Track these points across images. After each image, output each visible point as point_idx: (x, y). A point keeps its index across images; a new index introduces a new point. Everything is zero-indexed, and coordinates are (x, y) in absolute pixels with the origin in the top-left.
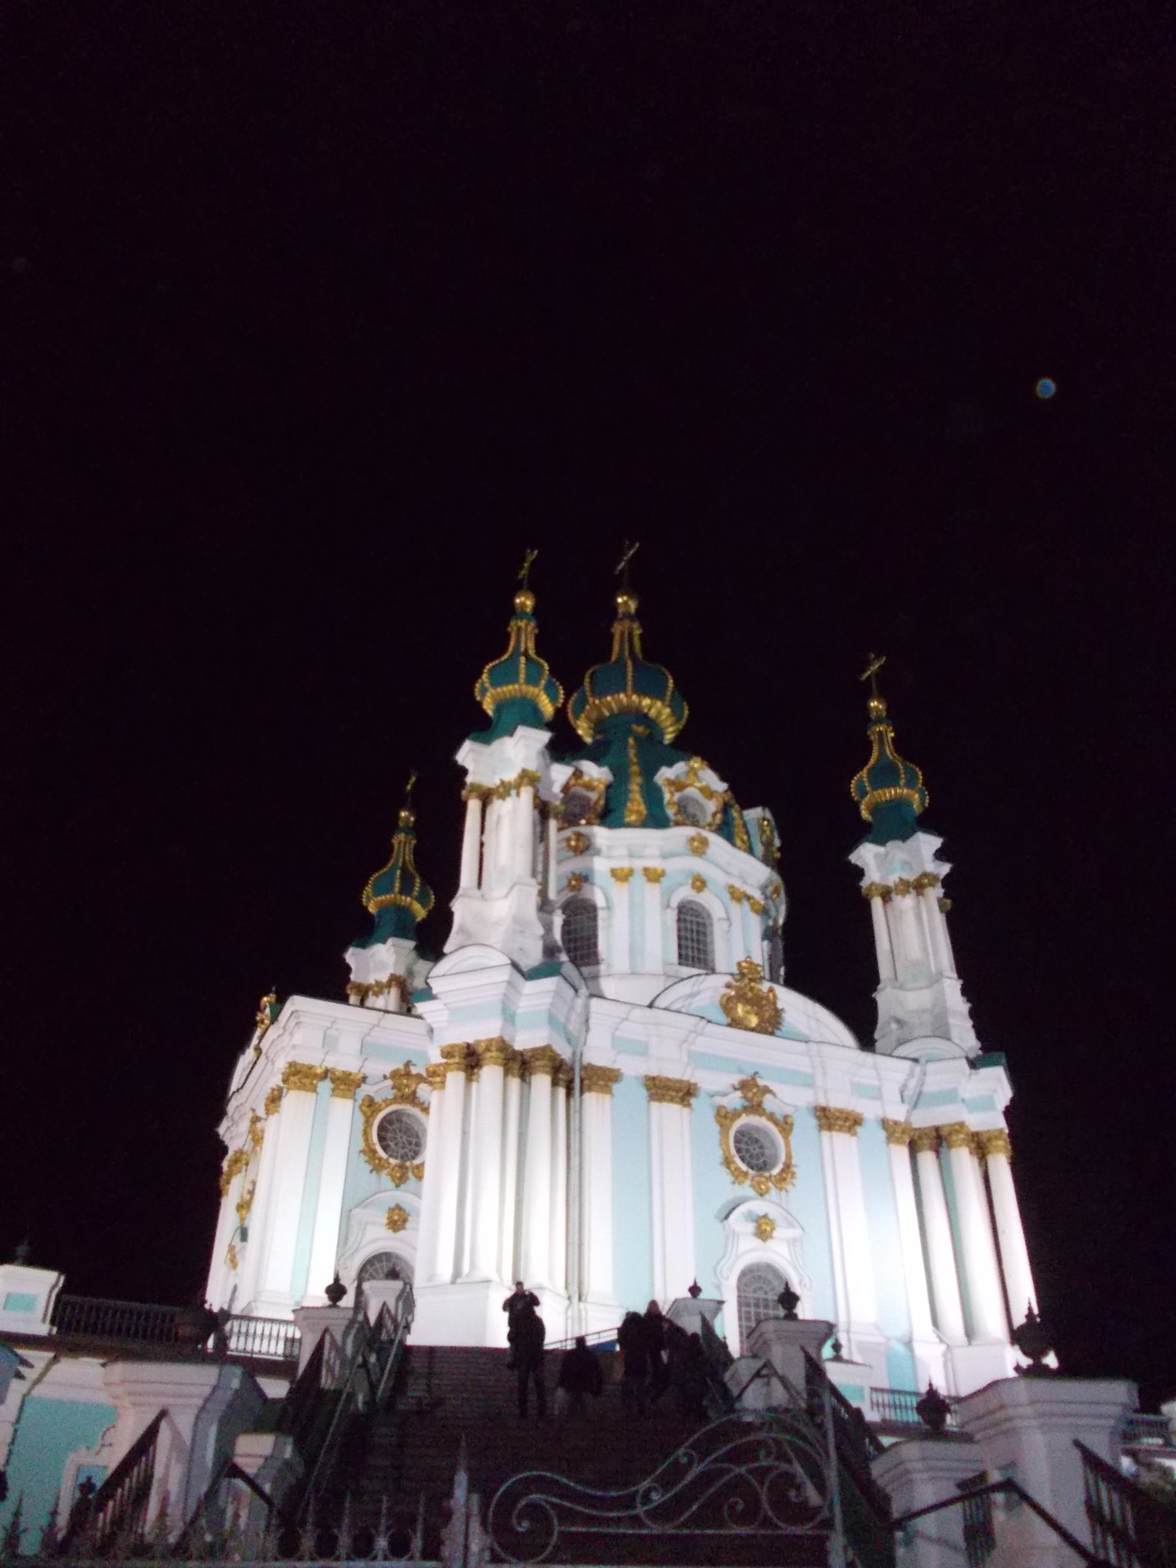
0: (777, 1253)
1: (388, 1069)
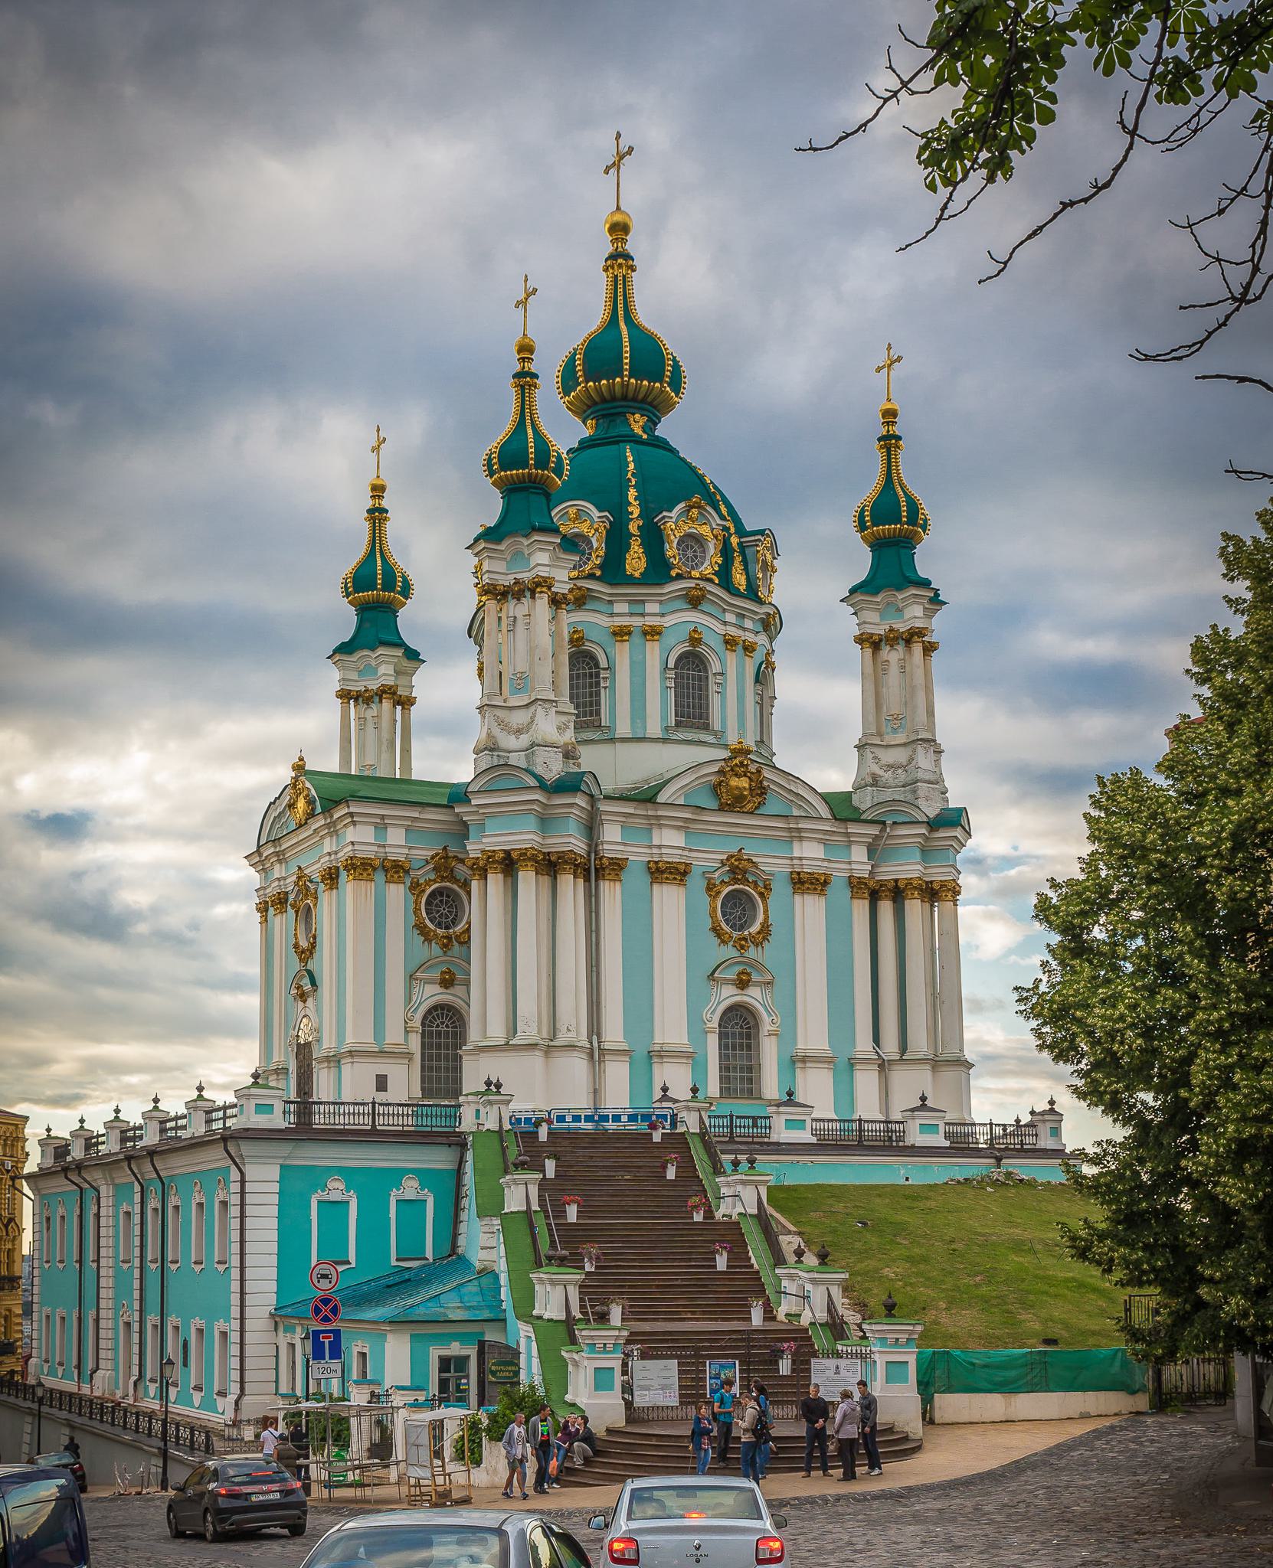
0: (754, 996)
1: (431, 853)
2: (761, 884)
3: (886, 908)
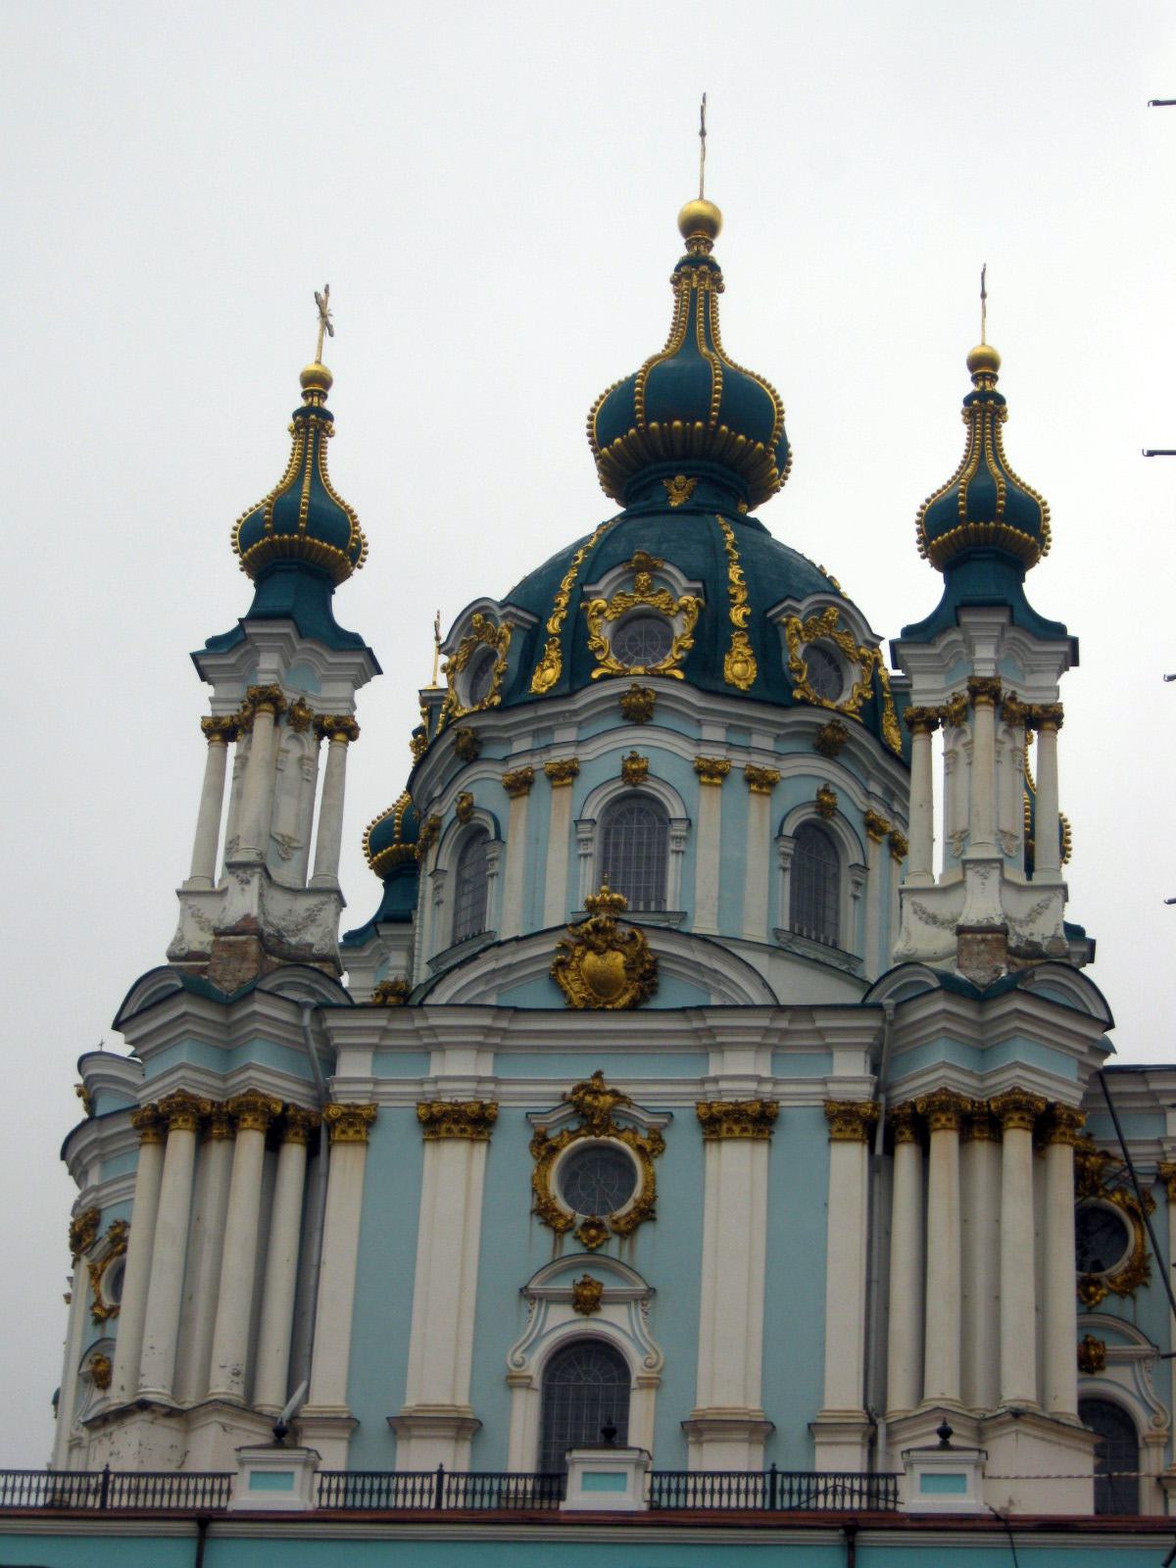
3: (906, 1156)
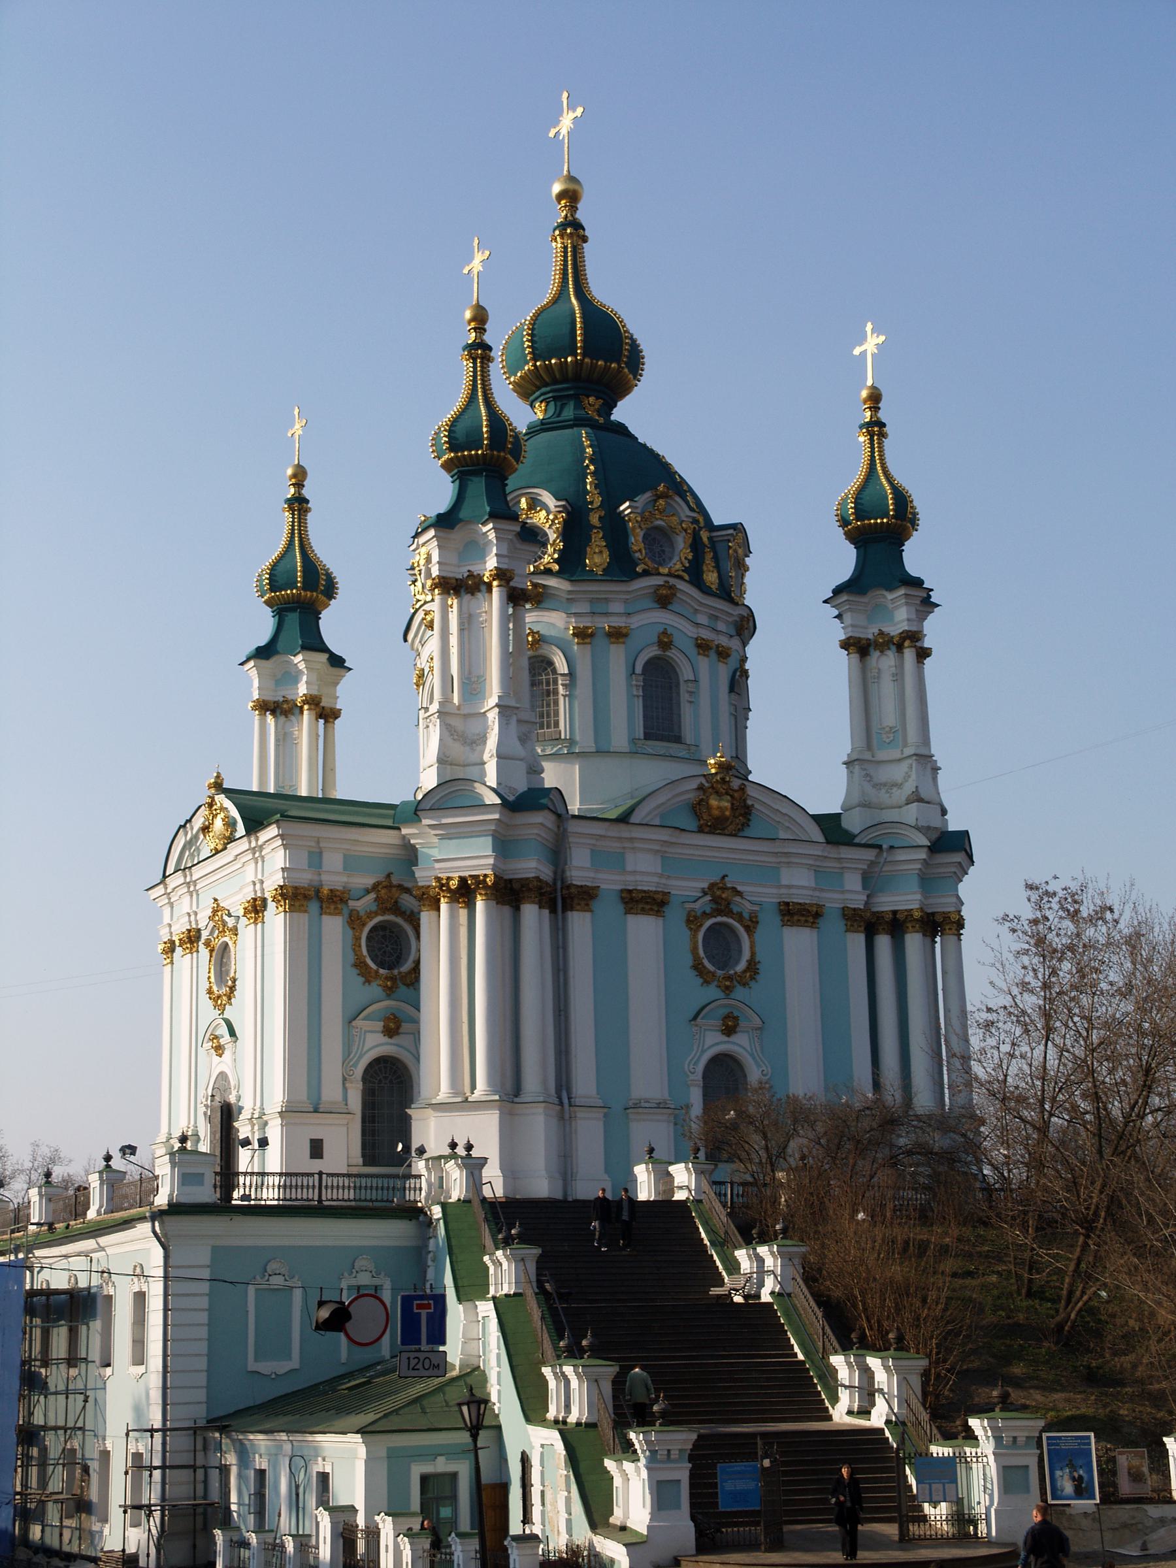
0: (740, 1045)
1: (369, 881)
2: (746, 915)
3: (883, 942)
